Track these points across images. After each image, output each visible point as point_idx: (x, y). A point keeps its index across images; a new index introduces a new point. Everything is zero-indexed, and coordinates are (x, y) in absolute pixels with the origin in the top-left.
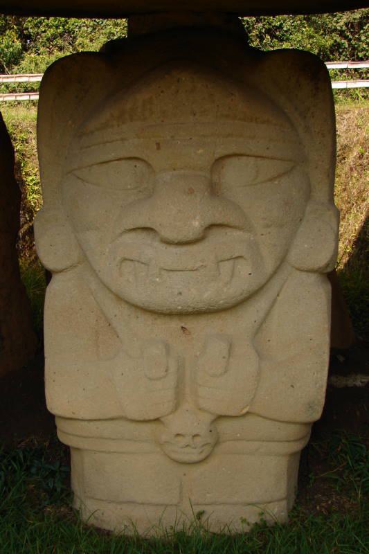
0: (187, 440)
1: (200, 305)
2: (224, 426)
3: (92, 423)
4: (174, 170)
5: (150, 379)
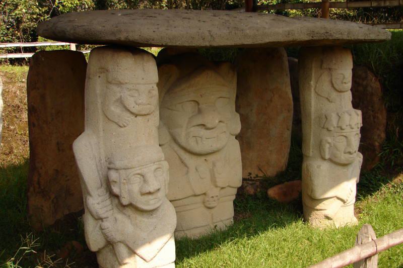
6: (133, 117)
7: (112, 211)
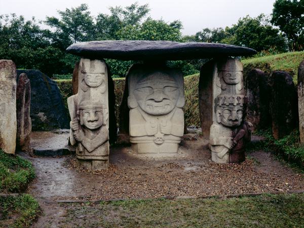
2: (167, 137)
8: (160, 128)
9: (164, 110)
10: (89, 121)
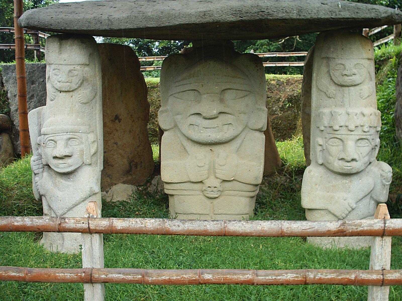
0: (212, 189)
1: (216, 140)
2: (227, 185)
3: (178, 184)
4: (208, 94)
5: (199, 167)
6: (59, 93)
7: (42, 169)
8: (214, 168)
9: (221, 134)
10: (55, 158)
